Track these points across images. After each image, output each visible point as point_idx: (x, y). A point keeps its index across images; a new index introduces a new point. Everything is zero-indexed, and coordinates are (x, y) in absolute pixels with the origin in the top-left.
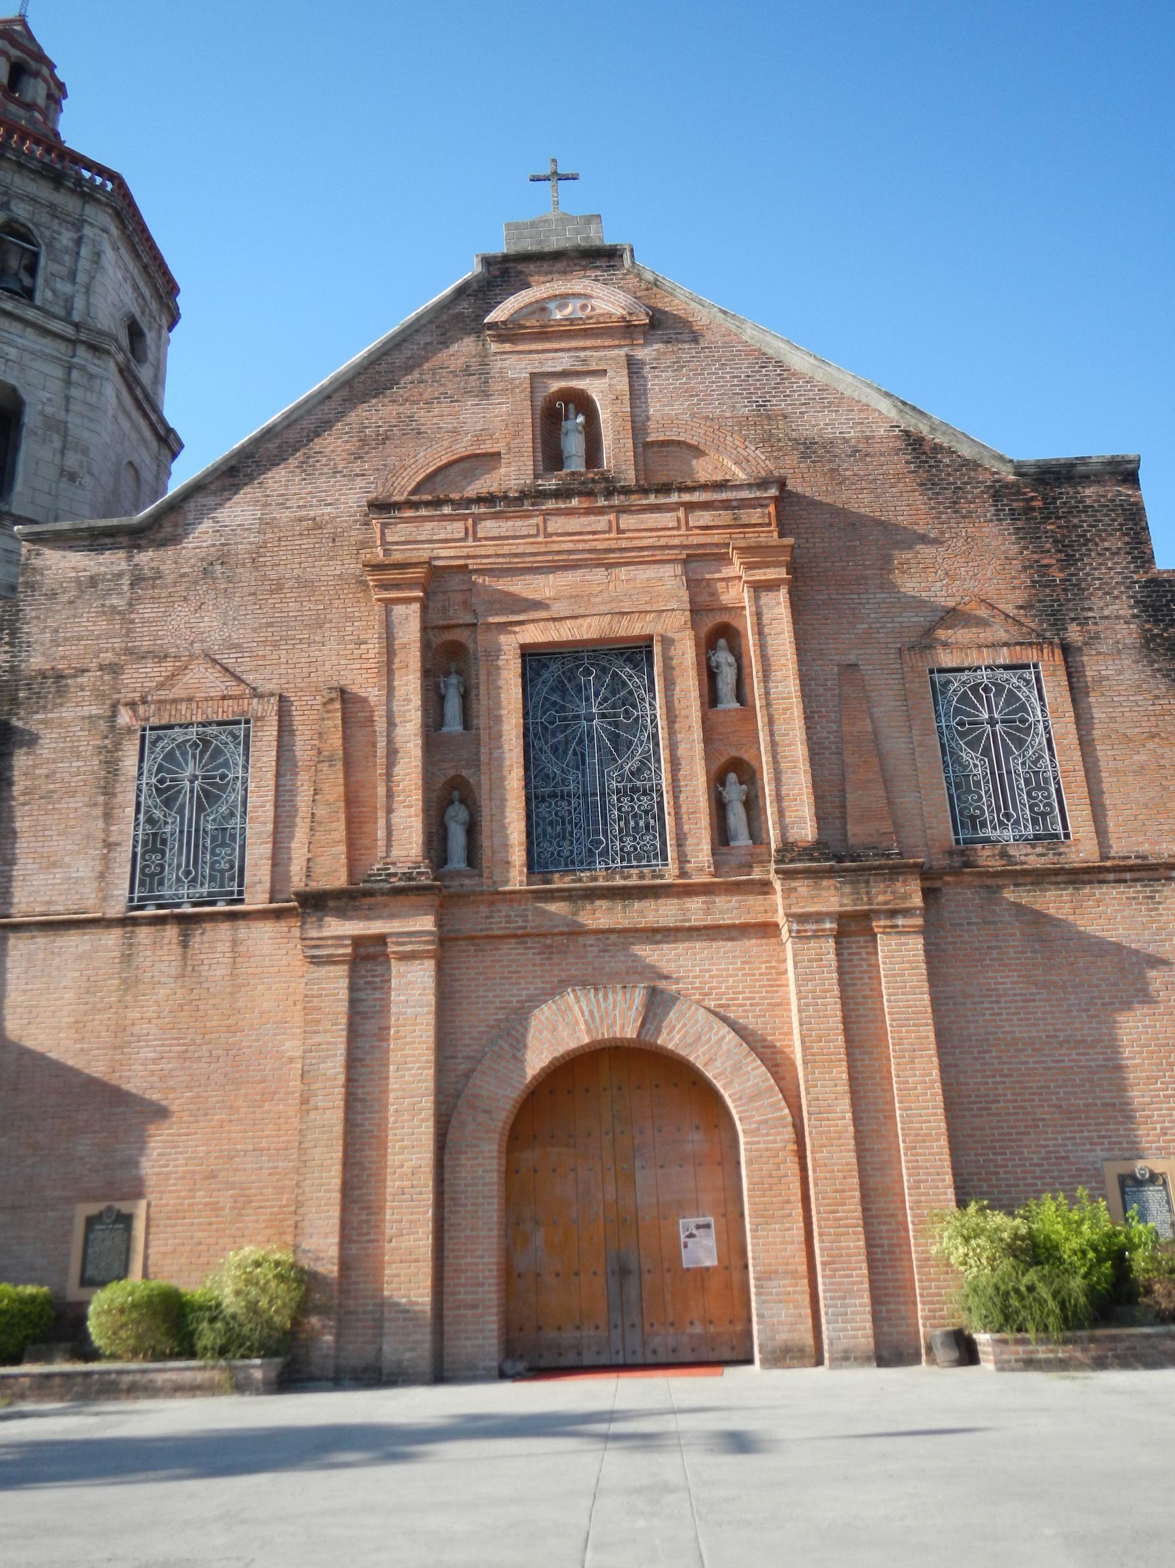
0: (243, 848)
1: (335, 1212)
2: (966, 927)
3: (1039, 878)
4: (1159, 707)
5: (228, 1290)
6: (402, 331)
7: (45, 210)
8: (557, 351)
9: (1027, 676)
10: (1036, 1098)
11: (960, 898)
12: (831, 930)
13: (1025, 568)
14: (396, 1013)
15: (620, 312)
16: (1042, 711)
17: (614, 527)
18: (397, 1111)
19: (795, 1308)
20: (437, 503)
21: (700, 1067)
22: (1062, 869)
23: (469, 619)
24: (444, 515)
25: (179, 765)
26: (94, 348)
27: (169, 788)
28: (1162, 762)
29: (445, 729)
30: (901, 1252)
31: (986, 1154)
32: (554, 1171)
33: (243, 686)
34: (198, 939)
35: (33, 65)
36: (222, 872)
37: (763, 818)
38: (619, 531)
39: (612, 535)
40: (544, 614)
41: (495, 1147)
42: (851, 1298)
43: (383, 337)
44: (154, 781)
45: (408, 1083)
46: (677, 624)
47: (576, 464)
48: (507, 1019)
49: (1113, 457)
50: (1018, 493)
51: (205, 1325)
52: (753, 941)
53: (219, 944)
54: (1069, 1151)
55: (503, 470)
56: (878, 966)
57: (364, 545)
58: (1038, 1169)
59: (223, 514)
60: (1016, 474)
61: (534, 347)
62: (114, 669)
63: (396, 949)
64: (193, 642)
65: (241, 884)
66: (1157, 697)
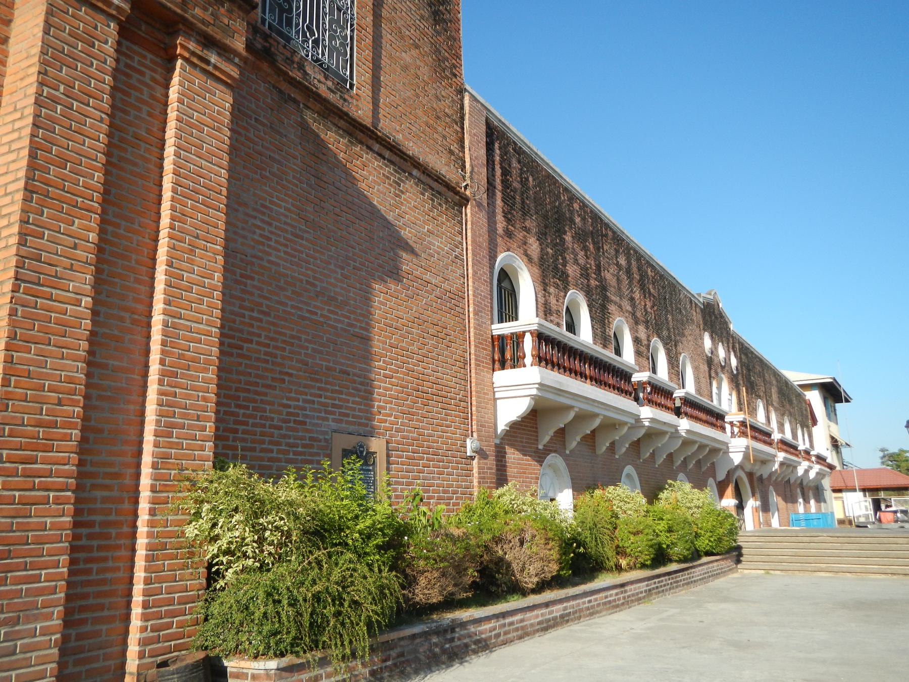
2: (253, 122)
4: (423, 27)
11: (254, 86)
22: (347, 114)
30: (119, 536)
31: (229, 405)
42: (28, 620)
54: (306, 416)
56: (166, 105)
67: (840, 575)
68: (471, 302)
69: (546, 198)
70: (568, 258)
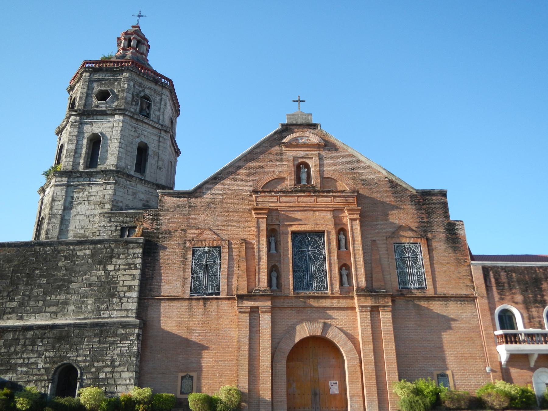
0: (220, 281)
1: (247, 377)
3: (420, 298)
5: (224, 396)
6: (261, 142)
7: (153, 91)
8: (300, 151)
9: (417, 246)
10: (418, 354)
12: (369, 310)
13: (418, 217)
14: (261, 327)
15: (317, 142)
16: (421, 255)
17: (315, 201)
18: (262, 352)
19: (359, 404)
20: (270, 192)
21: (336, 343)
23: (278, 223)
24: (272, 195)
25: (202, 257)
26: (165, 131)
27: (200, 264)
28: (450, 270)
29: (271, 252)
32: (298, 368)
33: (219, 237)
34: (208, 305)
35: (143, 40)
36: (215, 287)
37: (352, 279)
38: (317, 202)
39: (315, 203)
40: (297, 223)
41: (285, 362)
43: (255, 144)
44: (196, 262)
45: (264, 345)
46: (331, 228)
47: (304, 182)
48: (288, 329)
49: (441, 190)
50: (417, 197)
51: (219, 404)
52: (349, 311)
53: (214, 306)
55: (286, 183)
57: (250, 201)
58: (417, 372)
59: (213, 190)
60: (416, 192)
61: (294, 149)
62: (185, 231)
63: (261, 310)
64: (205, 225)
65: (219, 290)
66: (449, 253)
68: (482, 327)
69: (525, 277)
70: (544, 293)
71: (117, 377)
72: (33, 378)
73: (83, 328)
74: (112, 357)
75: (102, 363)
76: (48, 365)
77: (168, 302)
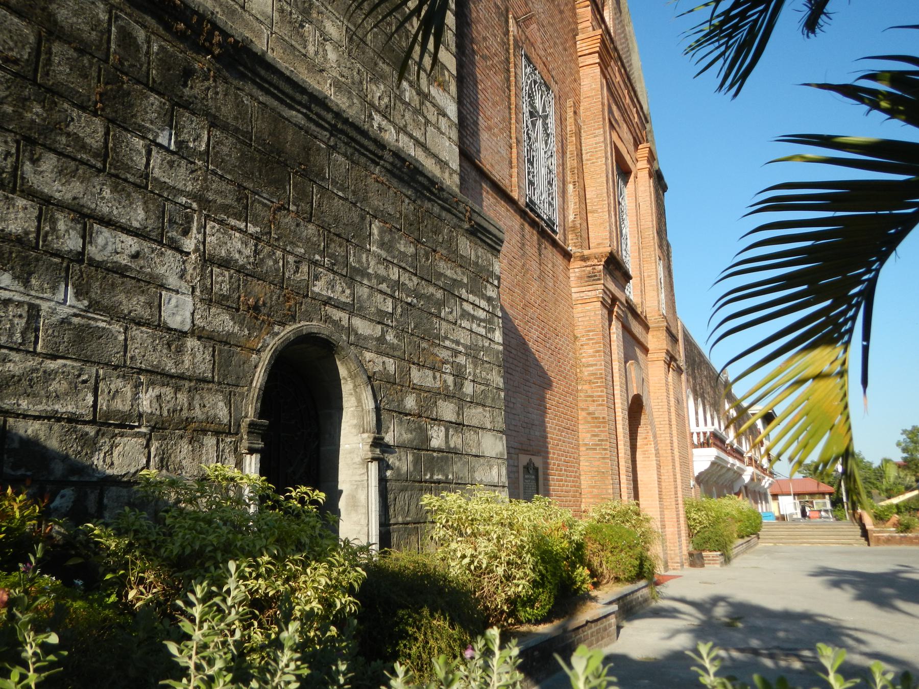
67: (815, 545)
71: (474, 452)
72: (135, 397)
73: (363, 160)
74: (456, 353)
75: (430, 373)
76: (223, 322)
77: (492, 195)
